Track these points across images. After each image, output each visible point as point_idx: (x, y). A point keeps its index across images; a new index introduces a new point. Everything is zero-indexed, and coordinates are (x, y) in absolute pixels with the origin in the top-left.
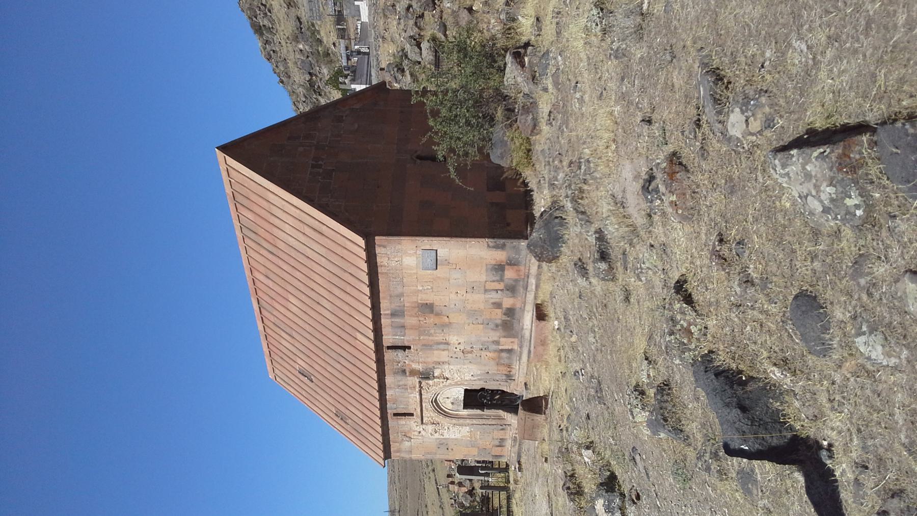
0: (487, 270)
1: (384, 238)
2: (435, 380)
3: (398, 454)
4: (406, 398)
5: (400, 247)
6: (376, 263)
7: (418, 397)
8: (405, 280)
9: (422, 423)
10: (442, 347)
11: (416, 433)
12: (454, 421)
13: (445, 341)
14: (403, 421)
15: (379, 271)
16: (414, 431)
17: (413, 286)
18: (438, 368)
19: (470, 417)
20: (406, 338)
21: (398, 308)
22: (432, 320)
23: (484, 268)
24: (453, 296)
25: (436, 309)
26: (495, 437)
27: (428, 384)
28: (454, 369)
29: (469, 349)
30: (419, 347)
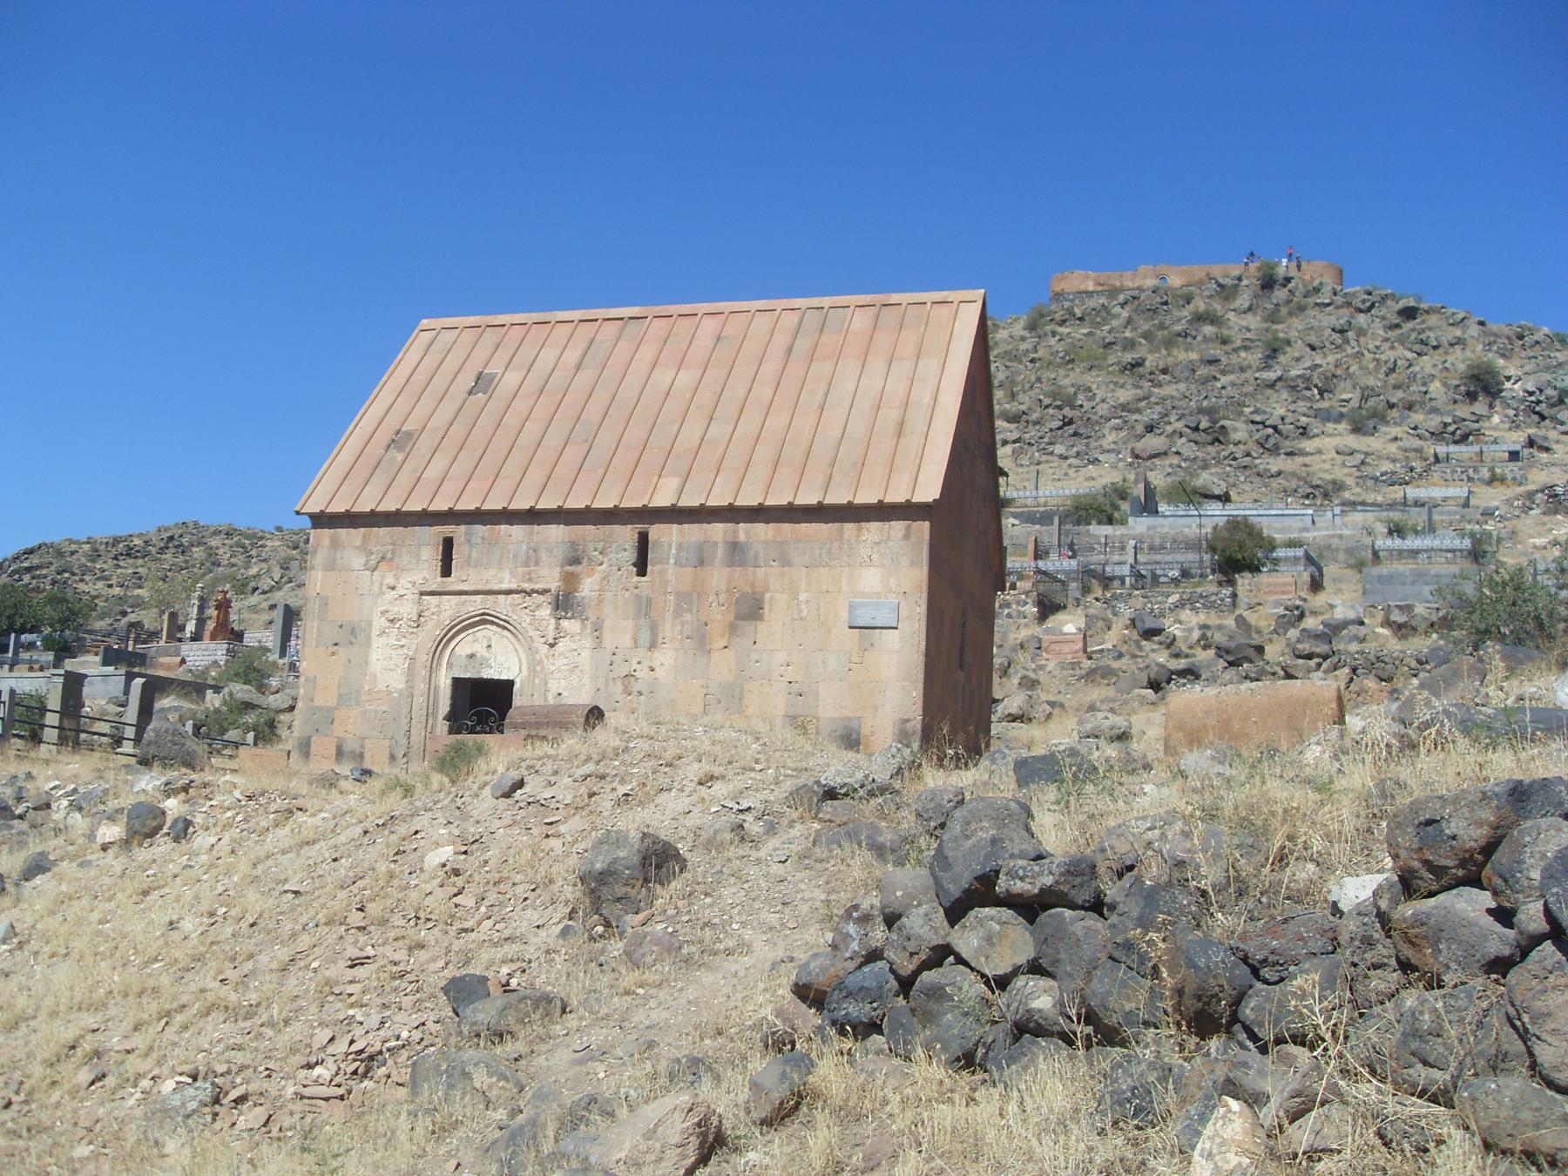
0: (844, 719)
1: (927, 537)
2: (553, 621)
3: (326, 542)
4: (500, 563)
5: (905, 562)
6: (868, 521)
7: (505, 586)
8: (823, 570)
9: (422, 593)
10: (645, 635)
11: (390, 580)
12: (423, 658)
13: (660, 641)
14: (431, 556)
15: (849, 528)
16: (397, 578)
17: (809, 584)
18: (584, 627)
19: (432, 689)
20: (671, 568)
21: (752, 553)
22: (719, 617)
23: (851, 715)
24: (780, 657)
25: (748, 626)
26: (368, 743)
27: (539, 606)
28: (577, 659)
29: (636, 687)
30: (646, 592)
